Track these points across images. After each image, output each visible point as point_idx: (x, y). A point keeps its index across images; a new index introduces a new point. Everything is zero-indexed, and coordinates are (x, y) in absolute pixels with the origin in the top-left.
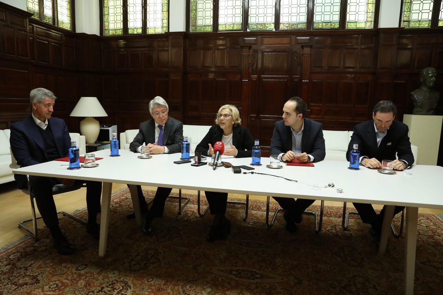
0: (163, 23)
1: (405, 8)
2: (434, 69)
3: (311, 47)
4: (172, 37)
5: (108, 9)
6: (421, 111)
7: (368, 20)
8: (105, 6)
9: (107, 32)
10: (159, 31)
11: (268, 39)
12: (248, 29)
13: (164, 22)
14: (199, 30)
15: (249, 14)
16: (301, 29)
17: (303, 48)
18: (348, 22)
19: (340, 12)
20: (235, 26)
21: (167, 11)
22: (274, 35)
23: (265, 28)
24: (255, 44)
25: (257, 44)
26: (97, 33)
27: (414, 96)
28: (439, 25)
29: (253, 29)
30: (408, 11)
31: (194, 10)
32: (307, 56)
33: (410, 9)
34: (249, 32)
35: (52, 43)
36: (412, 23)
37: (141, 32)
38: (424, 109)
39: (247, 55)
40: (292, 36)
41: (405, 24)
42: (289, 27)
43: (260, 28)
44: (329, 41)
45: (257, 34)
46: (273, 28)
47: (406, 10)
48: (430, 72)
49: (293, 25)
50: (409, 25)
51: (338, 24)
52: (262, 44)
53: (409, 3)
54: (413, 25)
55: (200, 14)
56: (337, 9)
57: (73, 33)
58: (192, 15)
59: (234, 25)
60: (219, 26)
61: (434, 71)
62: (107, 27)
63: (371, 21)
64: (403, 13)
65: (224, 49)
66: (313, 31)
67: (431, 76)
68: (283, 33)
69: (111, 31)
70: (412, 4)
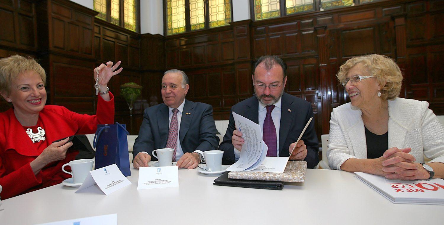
5: (171, 10)
8: (168, 7)
10: (223, 24)
13: (227, 14)
21: (229, 3)
26: (162, 33)
35: (118, 44)
43: (336, 6)
46: (352, 3)
57: (139, 34)
69: (174, 30)
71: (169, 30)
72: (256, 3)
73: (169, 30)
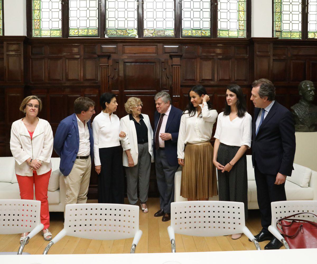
1: (276, 18)
2: (312, 82)
3: (180, 56)
4: (8, 42)
6: (303, 128)
7: (240, 29)
11: (130, 47)
12: (106, 35)
15: (107, 18)
17: (172, 58)
18: (220, 30)
19: (211, 19)
20: (90, 31)
22: (136, 42)
23: (126, 34)
24: (114, 53)
25: (117, 53)
27: (294, 112)
28: (309, 37)
29: (111, 35)
30: (279, 21)
31: (38, 10)
32: (176, 67)
33: (281, 19)
34: (107, 39)
36: (284, 33)
38: (305, 125)
39: (106, 65)
40: (158, 44)
41: (277, 34)
42: (155, 34)
43: (120, 35)
44: (200, 50)
45: (117, 40)
46: (136, 35)
47: (277, 20)
48: (308, 86)
49: (159, 31)
50: (281, 36)
51: (209, 31)
52: (124, 53)
53: (279, 13)
54: (286, 36)
55: (45, 15)
56: (207, 15)
58: (35, 14)
59: (88, 29)
60: (70, 30)
61: (312, 84)
63: (244, 30)
64: (274, 23)
65: (78, 58)
66: (183, 39)
67: (309, 90)
68: (149, 41)
70: (282, 14)
72: (35, 16)
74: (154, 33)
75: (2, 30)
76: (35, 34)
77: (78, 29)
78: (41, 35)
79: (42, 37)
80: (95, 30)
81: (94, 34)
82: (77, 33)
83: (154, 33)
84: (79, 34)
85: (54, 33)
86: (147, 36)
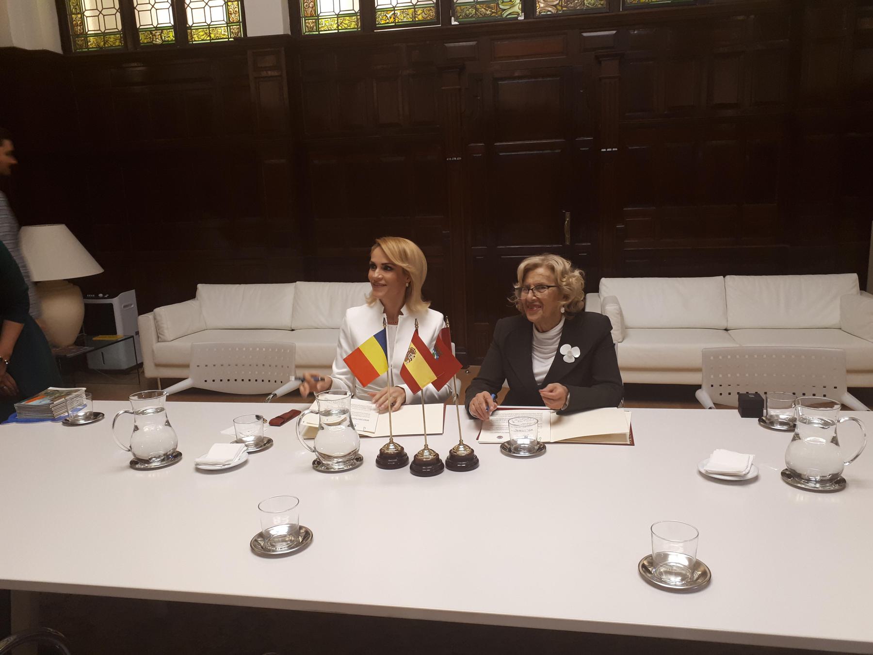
0: (228, 13)
9: (80, 42)
10: (223, 34)
12: (453, 18)
14: (326, 28)
16: (592, 9)
17: (600, 63)
23: (496, 13)
37: (174, 39)
59: (415, 8)
62: (79, 28)
71: (78, 36)
73: (78, 36)
74: (560, 4)
75: (241, 24)
76: (307, 28)
77: (394, 10)
78: (319, 28)
79: (321, 33)
80: (429, 8)
81: (428, 18)
82: (392, 18)
83: (560, 4)
84: (396, 21)
85: (344, 21)
86: (542, 13)
